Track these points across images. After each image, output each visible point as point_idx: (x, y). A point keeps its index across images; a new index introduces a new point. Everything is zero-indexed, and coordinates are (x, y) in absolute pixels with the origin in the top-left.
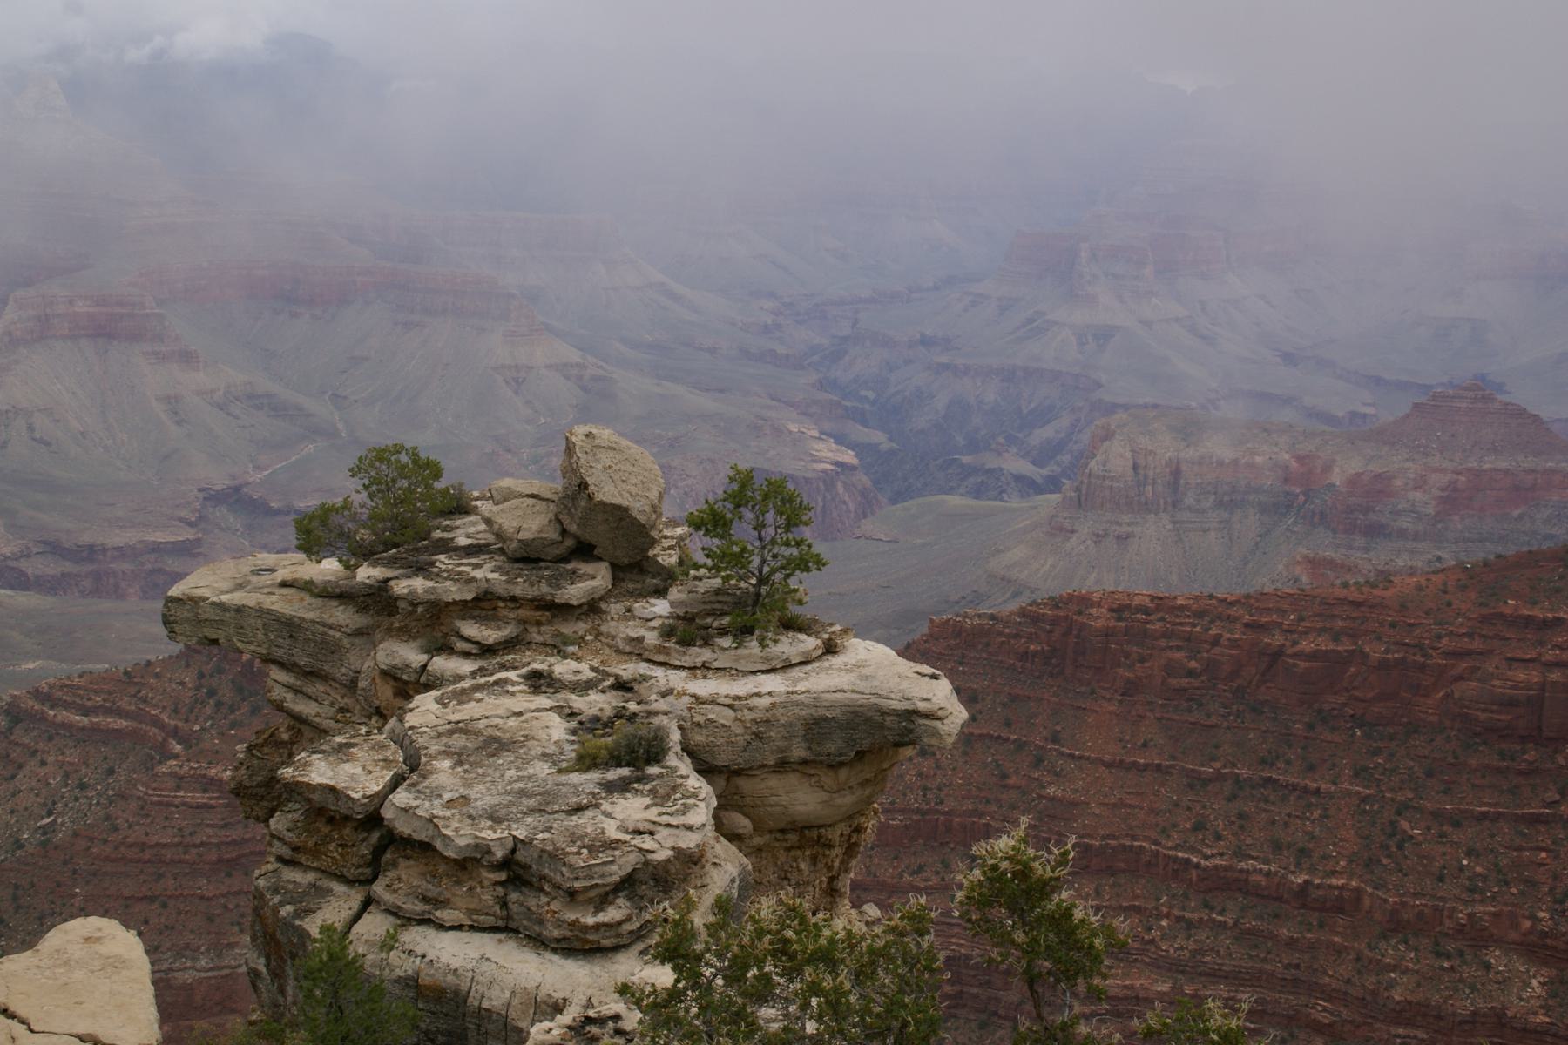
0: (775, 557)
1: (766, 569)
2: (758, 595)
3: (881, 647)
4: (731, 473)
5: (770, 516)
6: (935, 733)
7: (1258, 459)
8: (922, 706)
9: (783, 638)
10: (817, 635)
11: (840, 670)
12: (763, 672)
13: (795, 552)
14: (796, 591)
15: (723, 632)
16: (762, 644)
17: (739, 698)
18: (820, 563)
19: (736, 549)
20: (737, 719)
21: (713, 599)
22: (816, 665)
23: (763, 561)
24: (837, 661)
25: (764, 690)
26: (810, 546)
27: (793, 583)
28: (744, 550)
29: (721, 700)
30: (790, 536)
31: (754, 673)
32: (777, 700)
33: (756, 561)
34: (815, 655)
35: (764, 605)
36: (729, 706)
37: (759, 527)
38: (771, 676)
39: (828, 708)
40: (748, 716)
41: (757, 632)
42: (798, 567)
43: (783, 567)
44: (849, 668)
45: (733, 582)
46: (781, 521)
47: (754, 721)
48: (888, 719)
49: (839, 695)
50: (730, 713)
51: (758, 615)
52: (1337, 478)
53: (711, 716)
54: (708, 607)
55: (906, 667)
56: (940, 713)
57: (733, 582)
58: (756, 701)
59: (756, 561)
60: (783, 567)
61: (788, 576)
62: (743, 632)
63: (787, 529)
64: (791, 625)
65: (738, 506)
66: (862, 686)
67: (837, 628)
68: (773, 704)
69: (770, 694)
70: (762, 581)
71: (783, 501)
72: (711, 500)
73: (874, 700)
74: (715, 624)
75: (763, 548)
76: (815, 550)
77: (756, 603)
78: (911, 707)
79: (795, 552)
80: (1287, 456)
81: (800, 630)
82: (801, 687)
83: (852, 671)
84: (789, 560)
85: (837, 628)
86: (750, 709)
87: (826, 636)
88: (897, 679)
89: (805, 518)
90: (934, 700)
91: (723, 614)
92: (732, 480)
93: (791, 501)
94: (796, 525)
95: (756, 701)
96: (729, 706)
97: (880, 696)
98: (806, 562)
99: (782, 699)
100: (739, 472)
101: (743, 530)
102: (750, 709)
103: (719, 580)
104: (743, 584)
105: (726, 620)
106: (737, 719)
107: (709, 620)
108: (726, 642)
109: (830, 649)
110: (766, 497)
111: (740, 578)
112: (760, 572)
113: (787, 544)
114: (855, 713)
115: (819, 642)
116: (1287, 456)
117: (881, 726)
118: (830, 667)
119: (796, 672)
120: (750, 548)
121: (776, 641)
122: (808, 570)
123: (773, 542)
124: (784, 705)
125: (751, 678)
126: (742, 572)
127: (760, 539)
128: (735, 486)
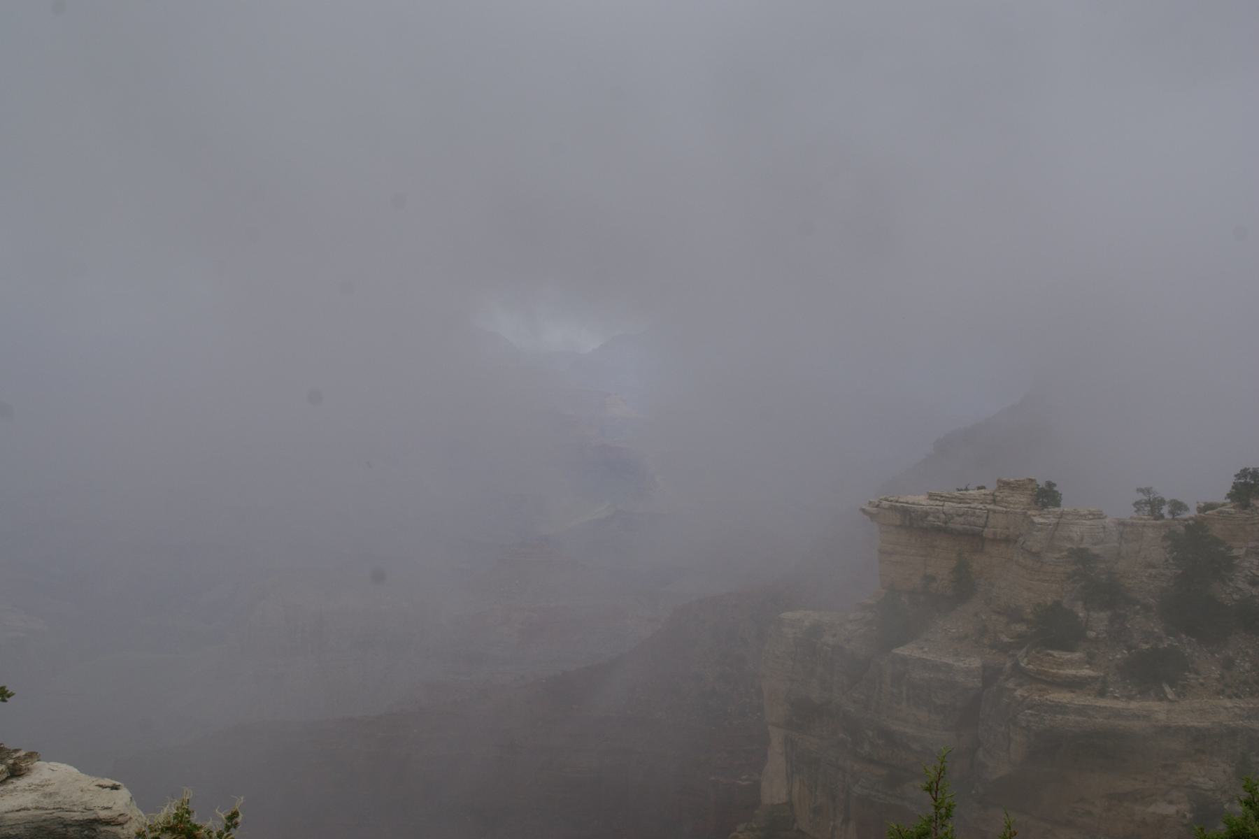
3: (64, 766)
8: (103, 814)
24: (21, 783)
39: (12, 827)
44: (31, 789)
48: (71, 829)
55: (88, 782)
56: (120, 819)
66: (45, 802)
67: (22, 753)
78: (93, 817)
87: (11, 762)
88: (80, 794)
90: (115, 808)
114: (39, 828)
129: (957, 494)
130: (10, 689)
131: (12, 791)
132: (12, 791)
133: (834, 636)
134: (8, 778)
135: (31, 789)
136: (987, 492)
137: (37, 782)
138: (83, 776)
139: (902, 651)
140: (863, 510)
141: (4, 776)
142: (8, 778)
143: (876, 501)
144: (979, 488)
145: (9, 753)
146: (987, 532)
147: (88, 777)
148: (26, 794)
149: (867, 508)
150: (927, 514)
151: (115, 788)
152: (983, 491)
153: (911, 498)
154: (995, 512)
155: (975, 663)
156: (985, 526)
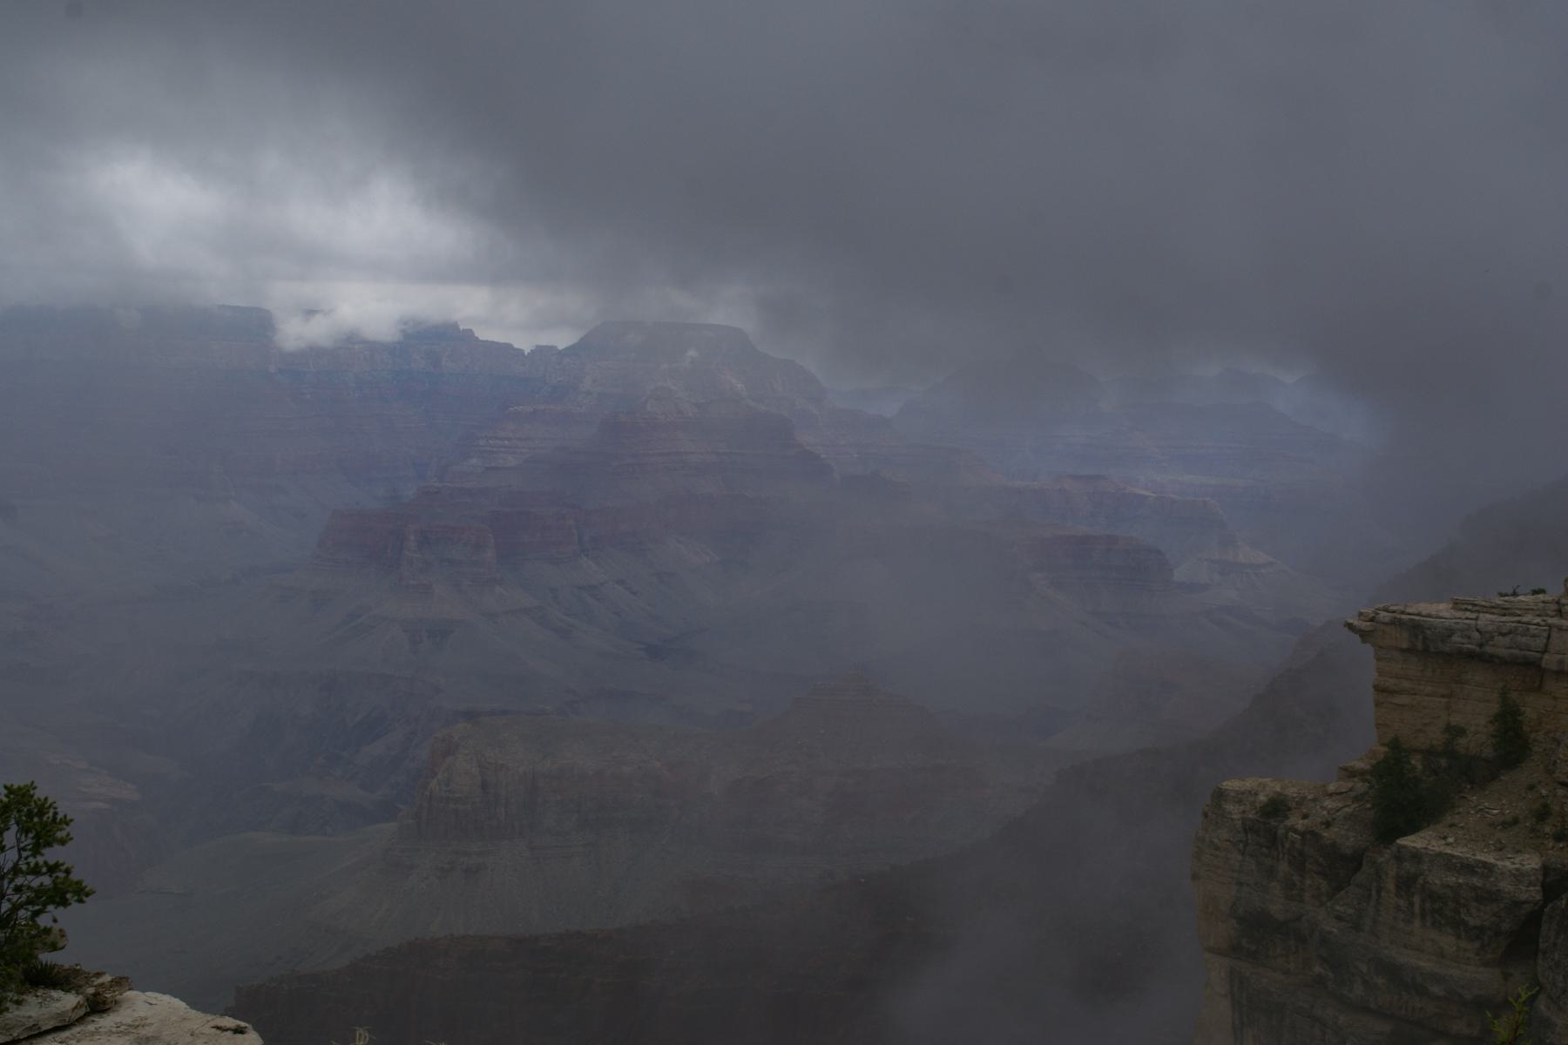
0: (18, 889)
3: (167, 998)
9: (30, 998)
10: (77, 989)
13: (46, 880)
14: (47, 931)
18: (81, 893)
22: (76, 1030)
24: (106, 1022)
26: (68, 872)
27: (44, 921)
30: (40, 860)
34: (75, 1016)
42: (51, 901)
43: (29, 902)
46: (28, 841)
60: (29, 902)
61: (36, 914)
63: (36, 851)
67: (107, 978)
71: (30, 815)
76: (74, 877)
79: (46, 880)
84: (39, 892)
87: (91, 990)
89: (59, 834)
93: (41, 813)
94: (49, 844)
98: (64, 891)
109: (97, 1006)
113: (36, 871)
115: (80, 998)
118: (97, 1031)
121: (19, 1003)
122: (64, 903)
123: (16, 870)
129: (1499, 601)
130: (88, 884)
131: (93, 1034)
132: (93, 1034)
133: (1305, 817)
134: (87, 1014)
135: (121, 1030)
136: (1547, 598)
137: (129, 1021)
139: (1411, 842)
140: (1350, 626)
141: (82, 1012)
142: (87, 1014)
143: (1369, 611)
144: (1535, 592)
145: (88, 978)
146: (1549, 661)
147: (200, 1014)
148: (113, 1038)
149: (1356, 622)
150: (1451, 632)
151: (239, 1031)
152: (1541, 596)
153: (1424, 608)
154: (1560, 629)
155: (1531, 862)
156: (1545, 651)
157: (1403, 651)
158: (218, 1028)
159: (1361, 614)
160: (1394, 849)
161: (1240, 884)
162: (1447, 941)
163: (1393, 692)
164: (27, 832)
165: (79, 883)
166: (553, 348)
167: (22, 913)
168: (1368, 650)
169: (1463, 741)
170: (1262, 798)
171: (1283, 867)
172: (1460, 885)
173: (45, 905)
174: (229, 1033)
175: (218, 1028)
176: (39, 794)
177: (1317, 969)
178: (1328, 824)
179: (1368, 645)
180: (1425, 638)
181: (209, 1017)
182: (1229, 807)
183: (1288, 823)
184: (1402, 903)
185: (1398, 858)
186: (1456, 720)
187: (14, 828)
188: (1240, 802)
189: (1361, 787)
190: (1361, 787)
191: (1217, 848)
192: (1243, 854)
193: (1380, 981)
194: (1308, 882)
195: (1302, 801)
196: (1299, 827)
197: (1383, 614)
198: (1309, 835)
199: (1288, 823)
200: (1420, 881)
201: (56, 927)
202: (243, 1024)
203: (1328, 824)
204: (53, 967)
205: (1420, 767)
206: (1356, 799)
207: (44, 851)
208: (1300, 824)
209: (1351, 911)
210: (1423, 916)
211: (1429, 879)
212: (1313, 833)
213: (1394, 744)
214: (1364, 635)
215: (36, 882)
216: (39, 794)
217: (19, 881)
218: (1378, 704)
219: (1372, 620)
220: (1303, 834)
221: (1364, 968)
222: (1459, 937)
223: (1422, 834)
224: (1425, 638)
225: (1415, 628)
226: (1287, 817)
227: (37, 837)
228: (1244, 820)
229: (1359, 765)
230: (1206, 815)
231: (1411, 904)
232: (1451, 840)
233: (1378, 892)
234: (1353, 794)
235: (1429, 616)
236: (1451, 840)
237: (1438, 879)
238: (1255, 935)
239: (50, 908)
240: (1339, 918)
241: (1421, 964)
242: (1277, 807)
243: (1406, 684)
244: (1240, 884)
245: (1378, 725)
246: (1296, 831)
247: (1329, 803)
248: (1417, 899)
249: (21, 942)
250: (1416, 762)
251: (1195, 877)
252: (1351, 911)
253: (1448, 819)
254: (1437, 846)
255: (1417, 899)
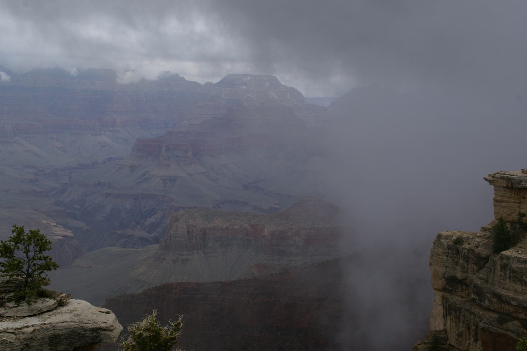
0: (34, 265)
1: (30, 271)
2: (27, 282)
3: (84, 301)
4: (13, 228)
5: (31, 248)
6: (109, 337)
7: (236, 227)
8: (103, 325)
9: (39, 301)
10: (54, 298)
11: (65, 313)
12: (29, 316)
13: (43, 262)
14: (44, 279)
15: (10, 300)
16: (29, 304)
17: (18, 329)
18: (55, 266)
19: (16, 262)
20: (17, 339)
21: (5, 285)
22: (54, 311)
23: (29, 267)
24: (64, 309)
25: (29, 324)
26: (50, 259)
27: (43, 275)
28: (20, 262)
29: (9, 331)
30: (41, 255)
31: (25, 317)
32: (36, 328)
33: (26, 267)
34: (53, 307)
35: (29, 287)
36: (13, 333)
37: (27, 252)
38: (34, 318)
39: (60, 330)
40: (22, 336)
41: (26, 299)
42: (45, 269)
43: (38, 269)
44: (69, 312)
45: (15, 277)
46: (37, 249)
47: (25, 339)
48: (88, 332)
49: (64, 324)
50: (13, 336)
51: (27, 291)
52: (266, 233)
53: (4, 339)
54: (3, 289)
55: (95, 309)
56: (111, 328)
57: (15, 277)
58: (26, 330)
59: (26, 267)
60: (38, 269)
61: (41, 273)
62: (19, 299)
63: (40, 252)
64: (43, 295)
65: (17, 243)
66: (76, 319)
67: (64, 295)
68: (34, 331)
69: (33, 326)
70: (29, 275)
71: (38, 240)
72: (4, 241)
73: (81, 325)
74: (6, 297)
75: (29, 261)
76: (53, 261)
77: (26, 286)
78: (98, 327)
79: (43, 262)
80: (247, 225)
81: (47, 297)
82: (48, 321)
83: (70, 313)
84: (41, 266)
85: (64, 295)
86: (23, 334)
87: (59, 299)
88: (91, 315)
89: (48, 247)
90: (108, 322)
91: (10, 292)
92: (13, 232)
93: (42, 240)
94: (44, 250)
95: (26, 330)
96: (13, 333)
97: (83, 323)
99: (39, 327)
100: (17, 228)
101: (19, 254)
102: (23, 334)
103: (8, 277)
104: (19, 278)
105: (12, 294)
106: (17, 339)
107: (3, 295)
108: (11, 304)
109: (61, 304)
110: (30, 238)
111: (18, 275)
112: (28, 271)
113: (40, 259)
114: (73, 331)
115: (55, 301)
116: (247, 225)
117: (84, 336)
119: (45, 315)
120: (22, 261)
121: (35, 302)
122: (50, 269)
123: (34, 258)
124: (39, 330)
125: (24, 320)
126: (19, 273)
127: (27, 257)
128: (15, 234)
130: (58, 263)
131: (60, 313)
132: (60, 313)
133: (469, 244)
134: (58, 306)
135: (69, 312)
137: (71, 309)
138: (93, 306)
139: (506, 253)
140: (485, 179)
141: (56, 306)
142: (58, 306)
143: (492, 173)
147: (95, 307)
148: (66, 314)
149: (488, 178)
150: (521, 181)
151: (108, 313)
157: (504, 187)
158: (101, 312)
159: (489, 175)
160: (500, 255)
161: (446, 267)
162: (518, 287)
163: (500, 202)
164: (37, 246)
165: (54, 263)
166: (212, 83)
167: (36, 272)
168: (492, 187)
169: (525, 219)
170: (454, 238)
171: (461, 261)
172: (523, 268)
173: (43, 270)
174: (104, 314)
175: (101, 312)
176: (41, 233)
177: (473, 296)
178: (477, 247)
179: (492, 186)
180: (512, 183)
181: (98, 308)
182: (443, 241)
183: (463, 246)
184: (502, 274)
185: (502, 258)
186: (522, 211)
187: (33, 244)
188: (446, 239)
189: (489, 234)
190: (489, 234)
191: (439, 255)
192: (447, 256)
193: (494, 300)
194: (470, 266)
195: (468, 239)
196: (467, 248)
197: (497, 175)
198: (471, 250)
199: (463, 246)
200: (509, 266)
201: (47, 278)
202: (109, 310)
203: (477, 247)
204: (46, 291)
205: (509, 227)
206: (487, 238)
207: (43, 252)
208: (467, 247)
209: (484, 276)
210: (510, 278)
211: (512, 266)
212: (472, 250)
213: (501, 220)
214: (491, 182)
215: (40, 262)
216: (41, 233)
217: (35, 262)
218: (495, 206)
219: (493, 177)
220: (468, 250)
221: (489, 295)
222: (522, 285)
223: (510, 250)
224: (512, 183)
225: (509, 179)
226: (463, 244)
227: (40, 247)
228: (448, 245)
229: (488, 227)
230: (435, 243)
231: (506, 274)
232: (520, 252)
233: (494, 270)
234: (486, 236)
235: (513, 175)
236: (520, 252)
237: (515, 265)
238: (452, 284)
239: (45, 271)
240: (480, 279)
241: (509, 294)
242: (459, 241)
243: (505, 199)
244: (446, 267)
245: (495, 213)
246: (466, 249)
247: (477, 240)
248: (508, 272)
249: (35, 282)
250: (508, 225)
251: (431, 264)
252: (484, 276)
253: (519, 245)
254: (515, 254)
255: (508, 272)
